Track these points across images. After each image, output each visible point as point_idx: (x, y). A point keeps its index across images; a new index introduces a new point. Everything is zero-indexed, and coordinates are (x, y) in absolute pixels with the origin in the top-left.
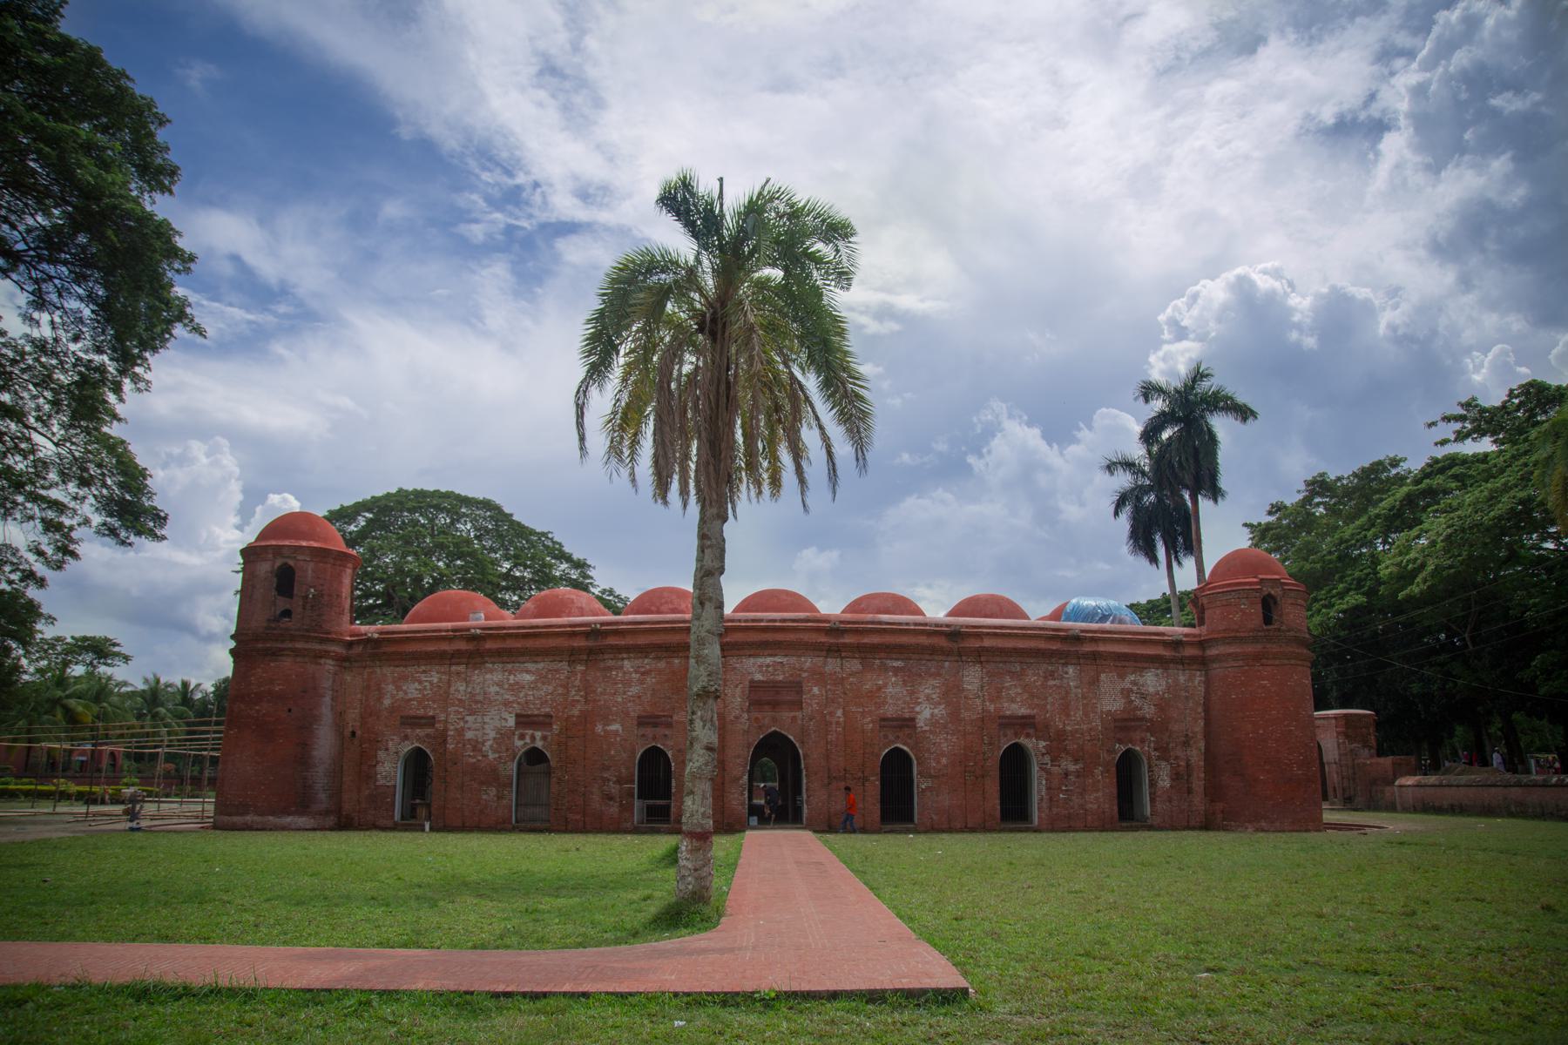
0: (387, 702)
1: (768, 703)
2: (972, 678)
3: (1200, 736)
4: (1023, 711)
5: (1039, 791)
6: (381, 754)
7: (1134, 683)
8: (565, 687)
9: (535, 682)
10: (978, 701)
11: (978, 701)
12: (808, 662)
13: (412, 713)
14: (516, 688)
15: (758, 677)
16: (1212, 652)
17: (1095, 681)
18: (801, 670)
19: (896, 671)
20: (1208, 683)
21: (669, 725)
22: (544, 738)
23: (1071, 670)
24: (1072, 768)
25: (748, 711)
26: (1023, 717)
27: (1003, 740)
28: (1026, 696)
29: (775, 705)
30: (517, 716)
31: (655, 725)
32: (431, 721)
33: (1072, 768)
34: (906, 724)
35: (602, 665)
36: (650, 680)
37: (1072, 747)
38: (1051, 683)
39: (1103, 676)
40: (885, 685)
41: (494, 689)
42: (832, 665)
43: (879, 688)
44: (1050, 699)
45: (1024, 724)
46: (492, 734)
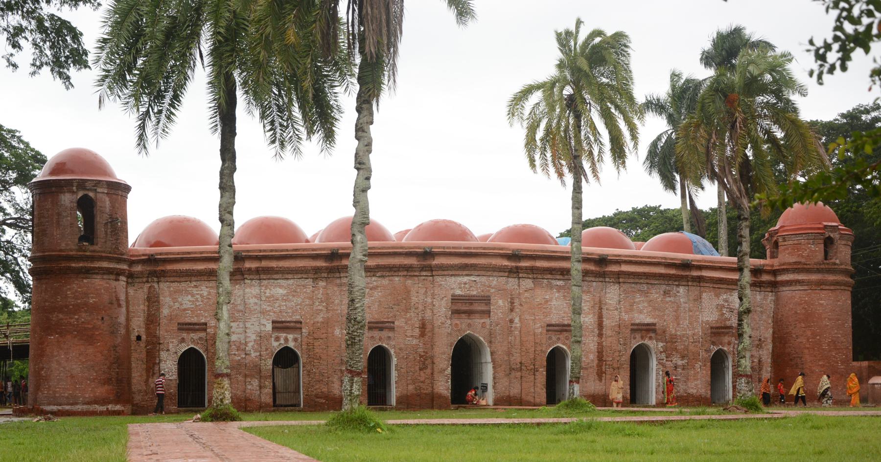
0: (165, 311)
1: (465, 312)
2: (612, 294)
3: (770, 340)
4: (648, 320)
5: (657, 380)
6: (163, 355)
7: (726, 301)
8: (311, 298)
9: (287, 295)
10: (616, 313)
11: (616, 313)
12: (495, 281)
13: (187, 320)
14: (272, 299)
15: (458, 292)
16: (780, 278)
17: (699, 299)
18: (490, 286)
19: (559, 288)
20: (777, 301)
21: (392, 329)
22: (295, 340)
23: (682, 290)
24: (680, 363)
25: (451, 319)
26: (648, 325)
28: (650, 309)
29: (470, 313)
30: (273, 322)
31: (381, 329)
32: (203, 327)
33: (680, 363)
35: (338, 281)
36: (377, 294)
37: (680, 347)
38: (668, 299)
39: (704, 295)
40: (551, 300)
41: (253, 301)
42: (512, 283)
43: (547, 301)
44: (667, 312)
45: (648, 329)
46: (253, 337)
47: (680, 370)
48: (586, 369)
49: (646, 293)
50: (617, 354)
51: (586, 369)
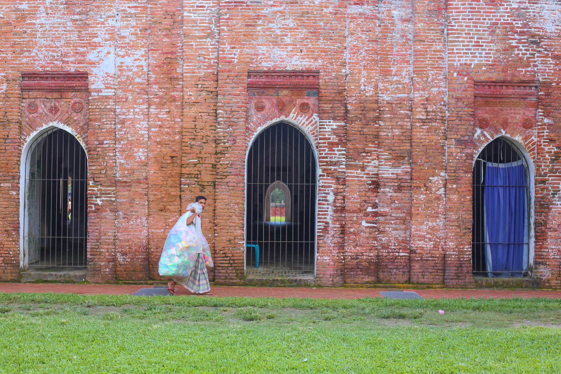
4: (296, 62)
24: (388, 172)
26: (294, 74)
27: (255, 116)
28: (303, 33)
33: (388, 172)
34: (70, 83)
37: (390, 131)
40: (33, 12)
43: (22, 17)
45: (303, 85)
47: (388, 191)
48: (127, 185)
50: (210, 148)
51: (127, 185)
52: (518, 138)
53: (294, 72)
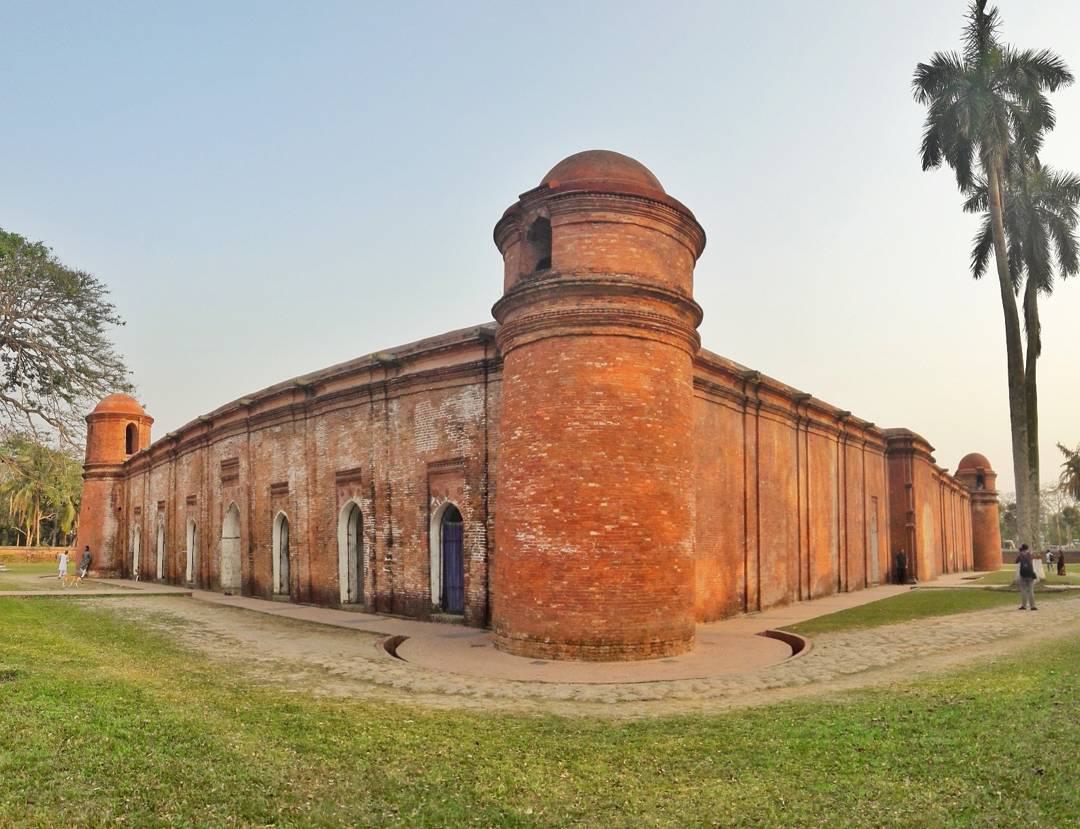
2: (320, 432)
7: (450, 410)
19: (278, 436)
24: (396, 532)
49: (349, 422)
52: (455, 503)
53: (353, 470)
